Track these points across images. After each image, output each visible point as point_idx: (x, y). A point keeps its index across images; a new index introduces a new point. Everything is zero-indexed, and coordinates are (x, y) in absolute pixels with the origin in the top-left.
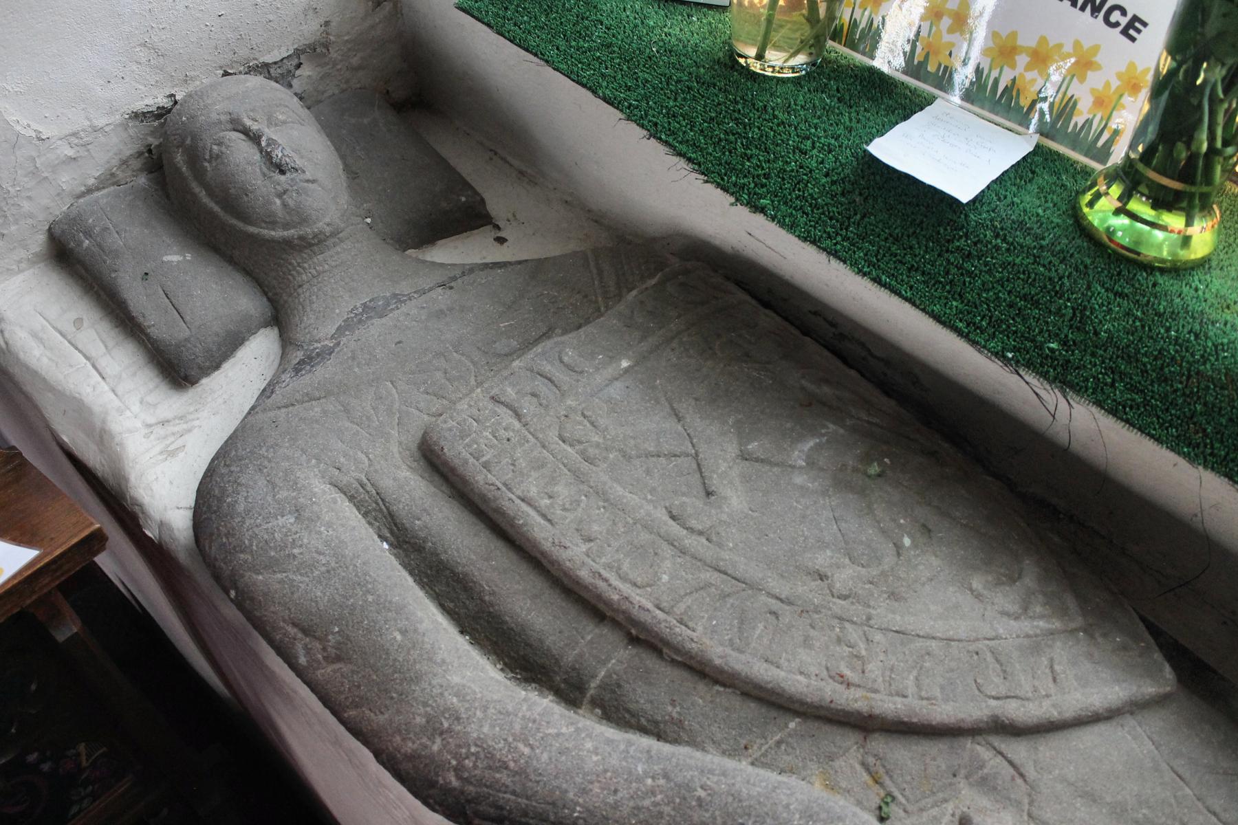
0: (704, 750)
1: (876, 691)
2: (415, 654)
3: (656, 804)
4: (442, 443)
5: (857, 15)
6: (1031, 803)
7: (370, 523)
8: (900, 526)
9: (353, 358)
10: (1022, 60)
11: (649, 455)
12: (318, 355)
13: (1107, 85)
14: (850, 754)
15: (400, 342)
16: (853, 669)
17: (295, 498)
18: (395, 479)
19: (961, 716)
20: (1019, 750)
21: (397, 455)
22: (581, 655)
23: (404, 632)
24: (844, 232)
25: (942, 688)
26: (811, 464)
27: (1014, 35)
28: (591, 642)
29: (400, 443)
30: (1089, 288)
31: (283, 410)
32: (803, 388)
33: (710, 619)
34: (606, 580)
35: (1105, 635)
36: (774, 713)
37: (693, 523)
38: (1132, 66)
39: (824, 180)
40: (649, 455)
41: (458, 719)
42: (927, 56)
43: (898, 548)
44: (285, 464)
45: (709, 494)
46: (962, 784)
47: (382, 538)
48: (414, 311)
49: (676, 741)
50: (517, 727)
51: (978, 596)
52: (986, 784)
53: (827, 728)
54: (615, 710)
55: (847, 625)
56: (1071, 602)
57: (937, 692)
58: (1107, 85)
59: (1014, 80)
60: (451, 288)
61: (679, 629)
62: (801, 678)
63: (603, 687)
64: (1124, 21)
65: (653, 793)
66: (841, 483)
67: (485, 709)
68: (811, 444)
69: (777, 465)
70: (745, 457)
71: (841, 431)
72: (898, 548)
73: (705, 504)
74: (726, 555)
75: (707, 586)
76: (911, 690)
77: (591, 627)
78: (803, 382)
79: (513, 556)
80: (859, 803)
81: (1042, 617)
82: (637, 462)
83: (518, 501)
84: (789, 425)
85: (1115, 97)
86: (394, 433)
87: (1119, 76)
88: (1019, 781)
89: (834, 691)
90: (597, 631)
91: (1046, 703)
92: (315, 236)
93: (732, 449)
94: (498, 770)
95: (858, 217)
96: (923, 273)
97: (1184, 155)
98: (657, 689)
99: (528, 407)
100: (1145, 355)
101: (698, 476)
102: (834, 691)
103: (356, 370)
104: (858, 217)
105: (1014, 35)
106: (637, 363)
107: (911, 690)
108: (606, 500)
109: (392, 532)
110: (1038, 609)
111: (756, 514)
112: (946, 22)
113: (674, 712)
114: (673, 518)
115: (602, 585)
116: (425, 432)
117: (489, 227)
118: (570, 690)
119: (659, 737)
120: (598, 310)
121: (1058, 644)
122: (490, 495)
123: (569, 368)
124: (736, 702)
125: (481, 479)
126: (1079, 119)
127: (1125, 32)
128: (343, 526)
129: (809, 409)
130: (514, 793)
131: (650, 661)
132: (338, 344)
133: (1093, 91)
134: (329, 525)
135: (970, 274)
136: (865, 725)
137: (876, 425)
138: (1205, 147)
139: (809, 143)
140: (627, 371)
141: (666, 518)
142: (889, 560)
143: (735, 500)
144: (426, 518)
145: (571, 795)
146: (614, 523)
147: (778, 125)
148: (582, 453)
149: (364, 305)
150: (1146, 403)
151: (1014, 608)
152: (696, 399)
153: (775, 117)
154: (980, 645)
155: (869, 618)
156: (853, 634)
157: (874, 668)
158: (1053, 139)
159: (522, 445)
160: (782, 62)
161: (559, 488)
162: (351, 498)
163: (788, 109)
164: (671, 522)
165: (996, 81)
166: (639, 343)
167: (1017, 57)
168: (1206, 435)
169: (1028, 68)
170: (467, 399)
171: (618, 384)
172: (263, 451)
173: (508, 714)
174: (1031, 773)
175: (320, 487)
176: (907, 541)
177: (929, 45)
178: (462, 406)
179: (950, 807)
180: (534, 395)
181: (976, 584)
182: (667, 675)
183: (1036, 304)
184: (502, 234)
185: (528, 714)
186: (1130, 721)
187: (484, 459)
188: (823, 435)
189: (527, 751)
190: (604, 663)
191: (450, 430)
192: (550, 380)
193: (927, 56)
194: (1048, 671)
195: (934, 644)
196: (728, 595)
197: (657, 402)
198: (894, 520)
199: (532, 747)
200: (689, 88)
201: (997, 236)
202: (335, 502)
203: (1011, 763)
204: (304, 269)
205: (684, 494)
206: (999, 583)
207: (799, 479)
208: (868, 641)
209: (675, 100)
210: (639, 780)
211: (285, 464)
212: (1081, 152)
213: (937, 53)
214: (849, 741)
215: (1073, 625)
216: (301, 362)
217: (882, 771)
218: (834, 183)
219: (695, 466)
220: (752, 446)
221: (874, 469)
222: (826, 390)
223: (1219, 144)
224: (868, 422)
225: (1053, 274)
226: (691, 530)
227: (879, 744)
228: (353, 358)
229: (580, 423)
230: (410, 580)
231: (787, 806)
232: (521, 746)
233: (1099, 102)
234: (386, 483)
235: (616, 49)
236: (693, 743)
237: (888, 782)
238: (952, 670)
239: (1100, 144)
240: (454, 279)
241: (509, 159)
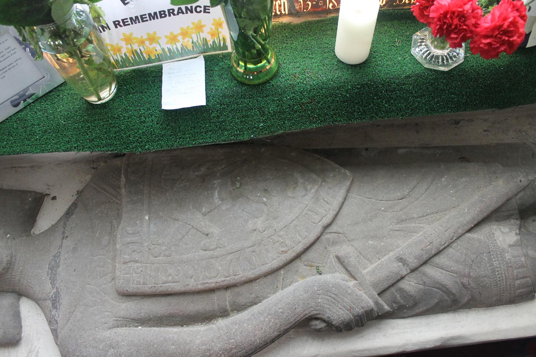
0: (268, 297)
1: (293, 247)
2: (182, 347)
3: (273, 323)
4: (125, 289)
5: (115, 58)
6: (346, 238)
7: (129, 327)
8: (259, 197)
9: (68, 288)
10: (180, 38)
11: (181, 239)
12: (55, 297)
13: (211, 29)
14: (299, 265)
15: (75, 270)
16: (284, 247)
17: (106, 344)
18: (123, 310)
19: (316, 234)
20: (334, 228)
21: (115, 303)
22: (218, 304)
23: (173, 344)
24: (178, 137)
25: (306, 231)
26: (222, 200)
27: (172, 33)
28: (217, 299)
29: (112, 299)
30: (257, 101)
31: (68, 324)
32: (197, 176)
33: (241, 268)
34: (207, 283)
35: (328, 177)
36: (275, 274)
37: (212, 247)
38: (214, 20)
39: (158, 126)
40: (181, 239)
41: (210, 350)
42: (149, 55)
43: (264, 203)
44: (91, 338)
45: (207, 235)
46: (329, 248)
47: (137, 327)
48: (66, 256)
49: (260, 302)
50: (225, 338)
51: (293, 198)
52: (334, 243)
53: (290, 265)
54: (239, 308)
55: (272, 237)
56: (314, 176)
57: (306, 234)
58: (211, 29)
59: (182, 44)
60: (67, 237)
61: (236, 277)
62: (274, 261)
63: (231, 306)
64: (202, 9)
65: (270, 321)
66: (235, 198)
67: (213, 341)
68: (217, 193)
69: (215, 209)
70: (204, 215)
71: (220, 181)
72: (264, 203)
73: (209, 239)
74: (228, 248)
75: (231, 261)
76: (300, 239)
77: (213, 295)
78: (195, 174)
79: (176, 298)
80: (313, 275)
81: (311, 188)
82: (181, 244)
83: (163, 285)
84: (206, 193)
85: (216, 31)
86: (107, 298)
87: (213, 24)
88: (340, 235)
89: (285, 257)
90: (216, 295)
91: (331, 212)
92: (7, 264)
93: (200, 216)
94: (231, 351)
95: (178, 129)
96: (210, 131)
97: (256, 52)
98: (244, 294)
99: (136, 256)
100: (286, 108)
101: (199, 232)
102: (285, 257)
103: (74, 291)
104: (178, 129)
105: (172, 33)
106: (150, 214)
107: (300, 239)
108: (185, 263)
109: (138, 323)
110: (309, 187)
111: (223, 229)
112: (147, 43)
113: (253, 295)
114: (205, 250)
115: (207, 285)
116: (117, 291)
117: (46, 198)
118: (224, 314)
119: (256, 304)
120: (117, 203)
121: (321, 192)
122: (154, 290)
123: (134, 234)
124: (265, 279)
125: (147, 289)
126: (210, 43)
127: (205, 12)
128: (126, 337)
129: (204, 181)
130: (240, 351)
131: (236, 290)
132: (57, 288)
133: (208, 33)
134: (123, 341)
135: (223, 122)
136: (298, 256)
137: (225, 167)
138: (260, 47)
139: (143, 117)
140: (149, 219)
141: (204, 252)
142: (265, 209)
143: (215, 230)
144: (143, 311)
145: (253, 339)
146: (193, 267)
147: (128, 118)
148: (165, 255)
149: (49, 268)
150: (296, 121)
151: (303, 193)
152: (176, 210)
153: (125, 116)
154: (305, 211)
155: (275, 230)
156: (275, 238)
157: (288, 242)
158: (207, 52)
159: (147, 269)
160: (107, 94)
161: (170, 271)
162: (118, 327)
163: (126, 111)
164: (207, 252)
165: (177, 48)
166: (143, 206)
167: (178, 38)
168: (316, 118)
169: (183, 38)
170: (117, 270)
171: (152, 225)
172: (80, 341)
173: (220, 337)
174: (341, 230)
175: (107, 334)
176: (265, 199)
177: (147, 52)
178: (118, 273)
179: (331, 256)
180: (133, 252)
181: (290, 195)
182: (243, 289)
183: (247, 116)
184: (52, 196)
185: (224, 332)
186: (350, 194)
187: (142, 282)
188: (216, 187)
189: (233, 341)
190: (226, 300)
191: (123, 283)
192: (133, 243)
193: (149, 55)
194: (325, 203)
195: (295, 222)
196: (239, 258)
197: (167, 220)
198: (256, 196)
199: (233, 339)
200: (89, 127)
201: (221, 105)
202: (116, 333)
203: (335, 233)
204: (15, 275)
205: (201, 241)
206: (295, 188)
207: (224, 208)
208: (280, 236)
209: (88, 135)
210: (264, 321)
211: (91, 338)
212: (218, 51)
213: (151, 53)
214: (298, 263)
215: (319, 183)
216: (53, 304)
217: (310, 263)
218: (162, 124)
219: (196, 230)
220: (204, 210)
221: (238, 185)
222: (203, 170)
223: (263, 43)
224: (222, 169)
225: (245, 105)
226: (213, 250)
227: (304, 257)
228: (68, 288)
229: (155, 248)
230: (156, 328)
231: (301, 295)
232: (231, 341)
233: (213, 35)
234: (122, 313)
235: (50, 131)
236: (265, 298)
237: (314, 264)
238: (305, 225)
239: (222, 45)
240: (64, 233)
241: (22, 165)
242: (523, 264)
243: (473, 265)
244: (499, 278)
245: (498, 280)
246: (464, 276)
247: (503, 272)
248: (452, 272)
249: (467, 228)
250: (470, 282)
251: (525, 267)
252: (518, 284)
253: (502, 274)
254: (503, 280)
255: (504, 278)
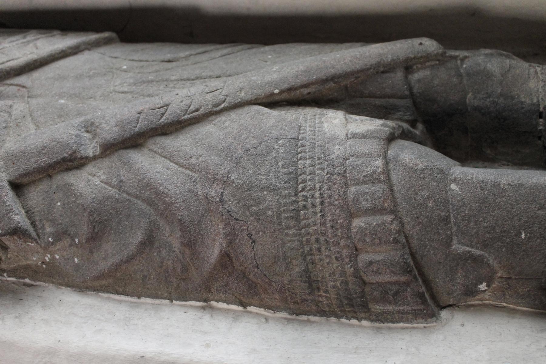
242: (374, 172)
243: (245, 158)
244: (305, 199)
245: (301, 203)
246: (214, 180)
247: (318, 186)
248: (192, 168)
249: (260, 92)
250: (226, 197)
251: (380, 181)
252: (360, 227)
253: (313, 189)
254: (313, 206)
255: (318, 201)
